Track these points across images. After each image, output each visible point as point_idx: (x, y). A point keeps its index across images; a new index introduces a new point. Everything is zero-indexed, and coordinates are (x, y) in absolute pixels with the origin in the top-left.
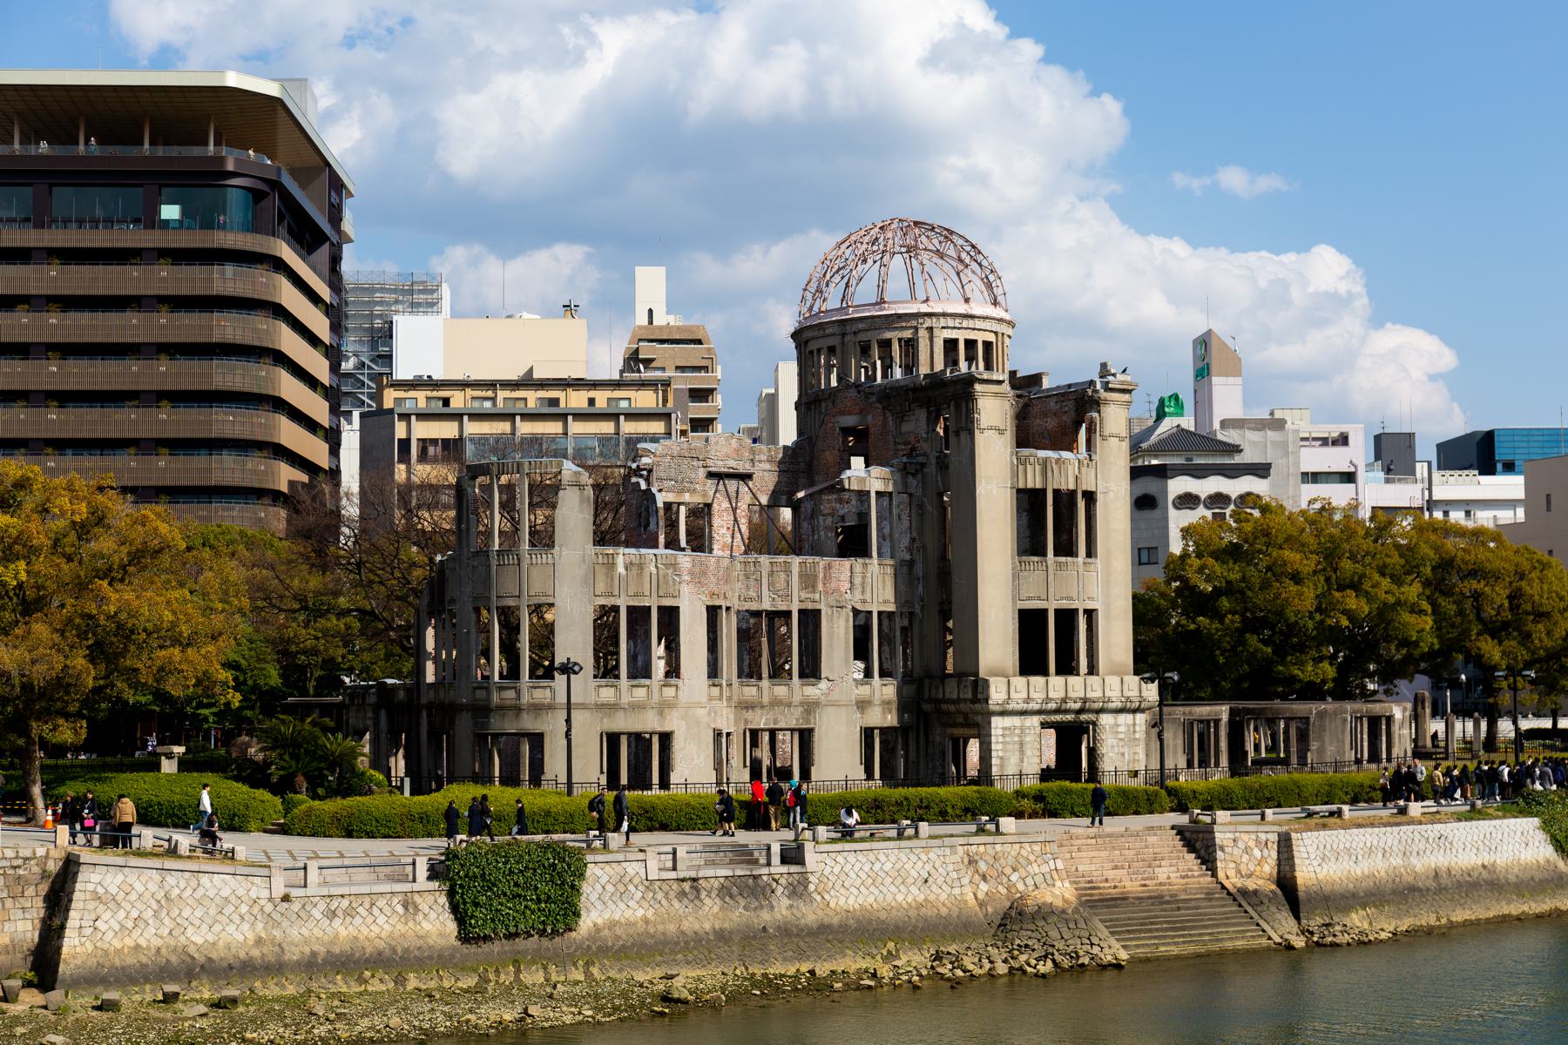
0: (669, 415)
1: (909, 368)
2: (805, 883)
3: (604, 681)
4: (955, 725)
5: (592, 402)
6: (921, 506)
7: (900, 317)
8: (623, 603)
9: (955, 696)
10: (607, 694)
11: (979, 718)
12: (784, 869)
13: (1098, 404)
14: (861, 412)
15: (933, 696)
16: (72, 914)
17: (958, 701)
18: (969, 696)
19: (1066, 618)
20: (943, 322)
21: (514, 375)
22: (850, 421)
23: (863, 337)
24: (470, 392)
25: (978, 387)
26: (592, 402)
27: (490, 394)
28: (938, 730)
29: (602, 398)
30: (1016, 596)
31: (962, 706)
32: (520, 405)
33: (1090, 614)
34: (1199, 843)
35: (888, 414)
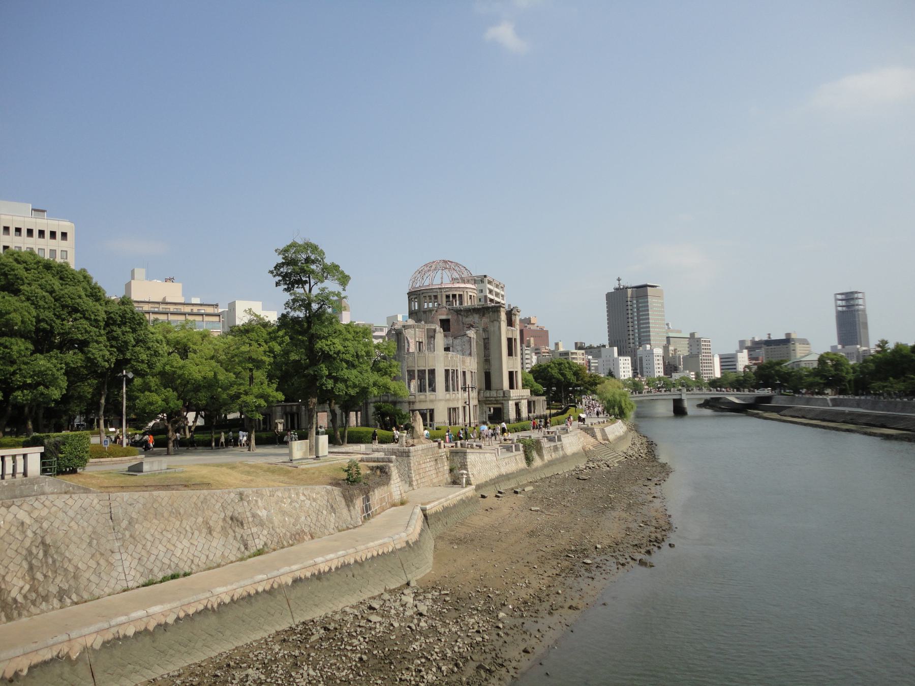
0: (219, 316)
1: (461, 303)
2: (562, 447)
3: (447, 392)
4: (492, 404)
5: (192, 310)
6: (477, 342)
7: (459, 288)
8: (450, 368)
9: (495, 396)
10: (448, 396)
11: (504, 402)
12: (559, 443)
13: (515, 315)
14: (447, 314)
15: (485, 396)
16: (469, 470)
17: (497, 397)
18: (502, 395)
19: (516, 372)
20: (468, 290)
21: (160, 300)
22: (444, 317)
23: (448, 293)
24: (150, 305)
25: (501, 309)
26: (192, 310)
27: (158, 306)
28: (484, 405)
29: (195, 309)
30: (508, 368)
31: (498, 399)
32: (168, 310)
33: (516, 372)
34: (589, 431)
35: (459, 316)
